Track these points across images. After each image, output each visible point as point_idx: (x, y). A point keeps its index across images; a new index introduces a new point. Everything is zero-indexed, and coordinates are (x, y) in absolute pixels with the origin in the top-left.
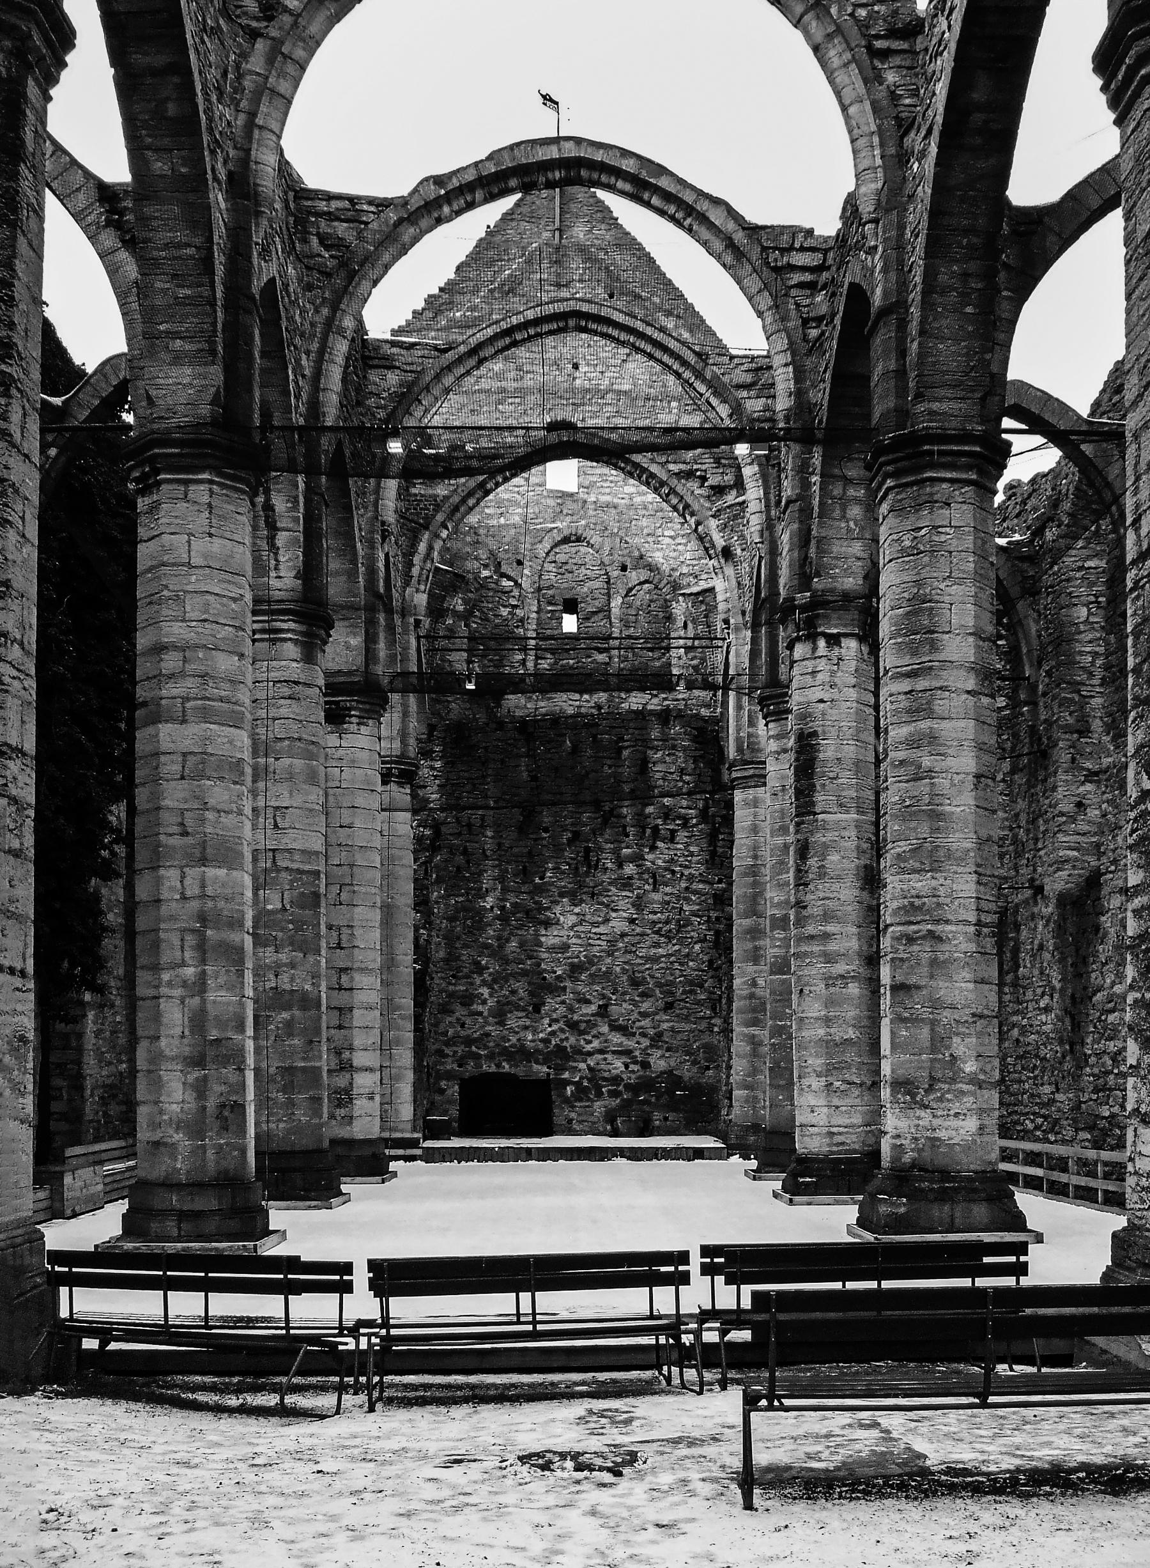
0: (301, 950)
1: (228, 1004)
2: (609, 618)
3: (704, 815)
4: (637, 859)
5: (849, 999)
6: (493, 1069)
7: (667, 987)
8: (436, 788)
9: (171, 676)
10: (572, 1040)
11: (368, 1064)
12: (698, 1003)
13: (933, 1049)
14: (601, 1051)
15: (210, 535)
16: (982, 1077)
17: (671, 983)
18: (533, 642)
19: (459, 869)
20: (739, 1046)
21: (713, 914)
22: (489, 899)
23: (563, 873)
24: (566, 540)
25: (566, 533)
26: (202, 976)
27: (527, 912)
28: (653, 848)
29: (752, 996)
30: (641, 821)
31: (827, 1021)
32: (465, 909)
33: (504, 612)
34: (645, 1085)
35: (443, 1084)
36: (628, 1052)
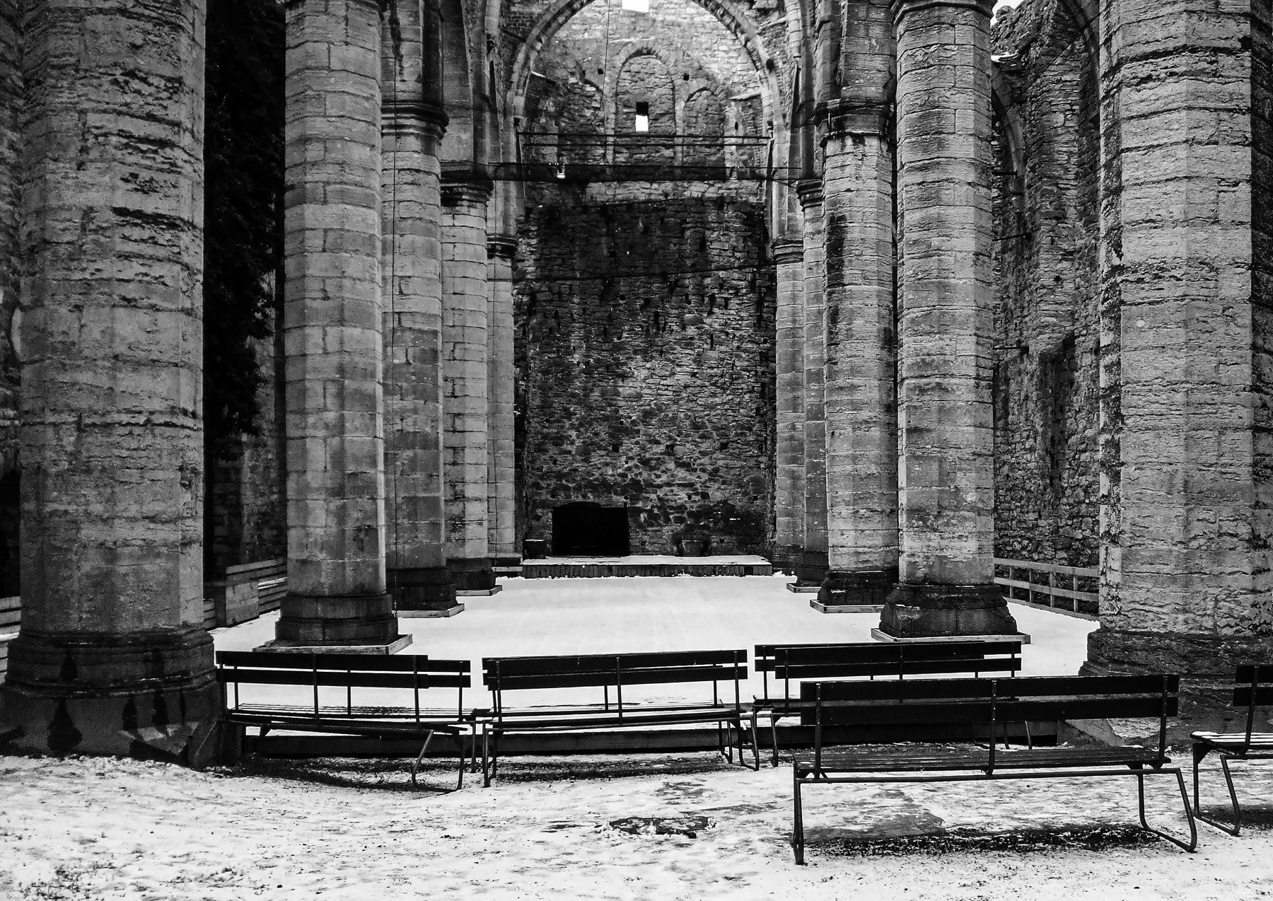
2: (674, 119)
3: (752, 286)
4: (698, 322)
5: (871, 440)
6: (580, 499)
7: (722, 430)
8: (532, 262)
10: (645, 475)
11: (478, 495)
12: (748, 443)
13: (942, 482)
14: (668, 484)
16: (980, 505)
17: (726, 427)
18: (611, 139)
19: (551, 330)
20: (782, 480)
21: (760, 369)
22: (576, 356)
23: (637, 334)
24: (639, 53)
25: (639, 46)
26: (342, 418)
27: (607, 367)
28: (710, 313)
29: (792, 438)
30: (701, 291)
31: (855, 459)
32: (556, 364)
33: (588, 113)
34: (705, 512)
35: (539, 512)
36: (691, 485)
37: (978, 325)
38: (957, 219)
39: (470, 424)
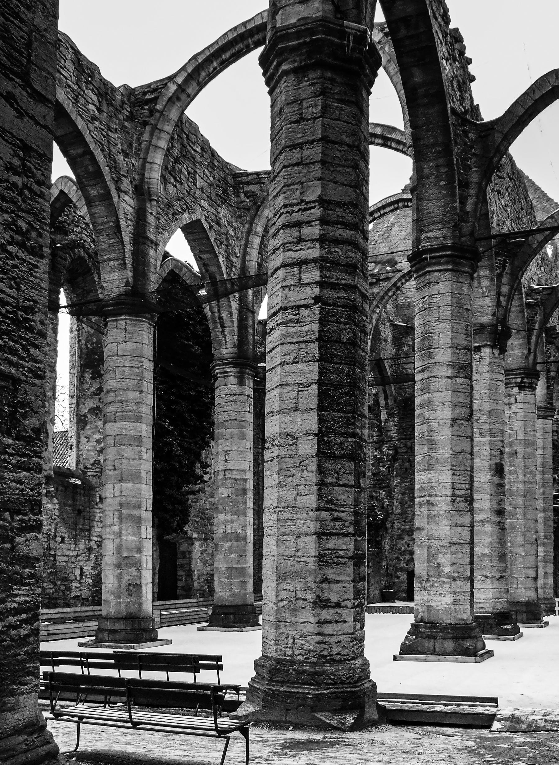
0: (236, 515)
1: (133, 541)
9: (111, 403)
13: (429, 561)
15: (126, 342)
19: (406, 469)
26: (121, 529)
35: (399, 573)
37: (454, 463)
38: (440, 400)
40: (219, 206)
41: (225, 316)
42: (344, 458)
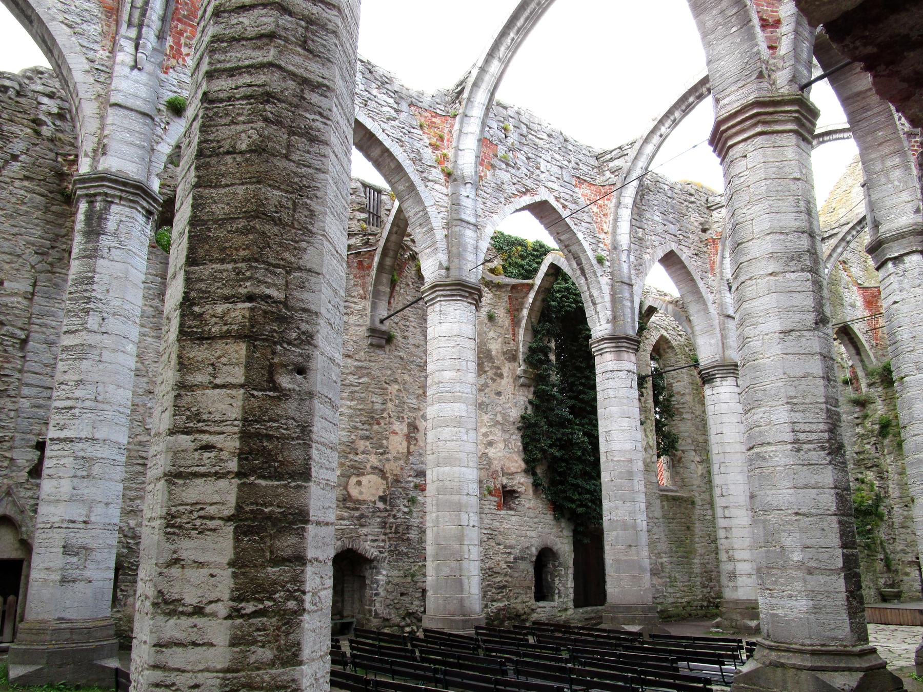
11: (745, 557)
35: (908, 570)
39: (733, 512)
40: (575, 186)
41: (595, 293)
42: (228, 338)
